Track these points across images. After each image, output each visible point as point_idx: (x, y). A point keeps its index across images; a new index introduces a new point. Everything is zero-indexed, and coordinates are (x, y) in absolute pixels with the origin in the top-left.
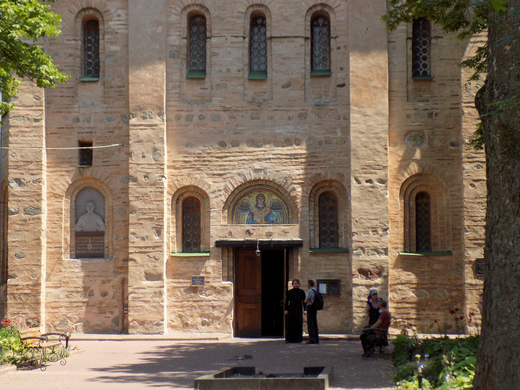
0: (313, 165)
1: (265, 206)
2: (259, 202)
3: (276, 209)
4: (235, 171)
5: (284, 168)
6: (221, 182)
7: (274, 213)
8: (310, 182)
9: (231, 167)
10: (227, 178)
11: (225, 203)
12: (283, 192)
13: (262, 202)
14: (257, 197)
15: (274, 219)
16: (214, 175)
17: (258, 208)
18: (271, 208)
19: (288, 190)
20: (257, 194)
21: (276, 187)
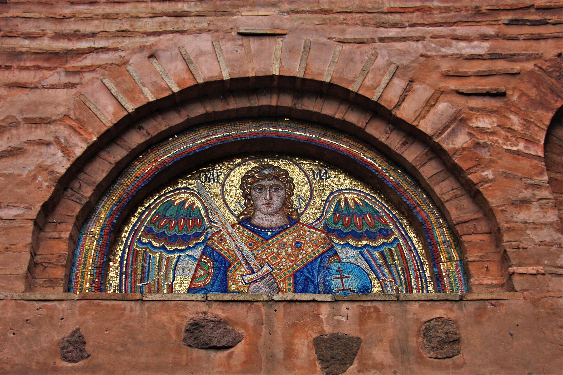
0: (535, 23)
1: (293, 220)
2: (261, 200)
3: (358, 237)
4: (127, 42)
5: (392, 32)
6: (53, 87)
7: (348, 254)
8: (533, 93)
9: (114, 26)
10: (92, 69)
11: (66, 183)
12: (394, 141)
13: (277, 203)
14: (248, 185)
15: (352, 283)
16: (16, 55)
17: (258, 230)
18: (328, 230)
19: (426, 126)
20: (243, 170)
21: (353, 118)
